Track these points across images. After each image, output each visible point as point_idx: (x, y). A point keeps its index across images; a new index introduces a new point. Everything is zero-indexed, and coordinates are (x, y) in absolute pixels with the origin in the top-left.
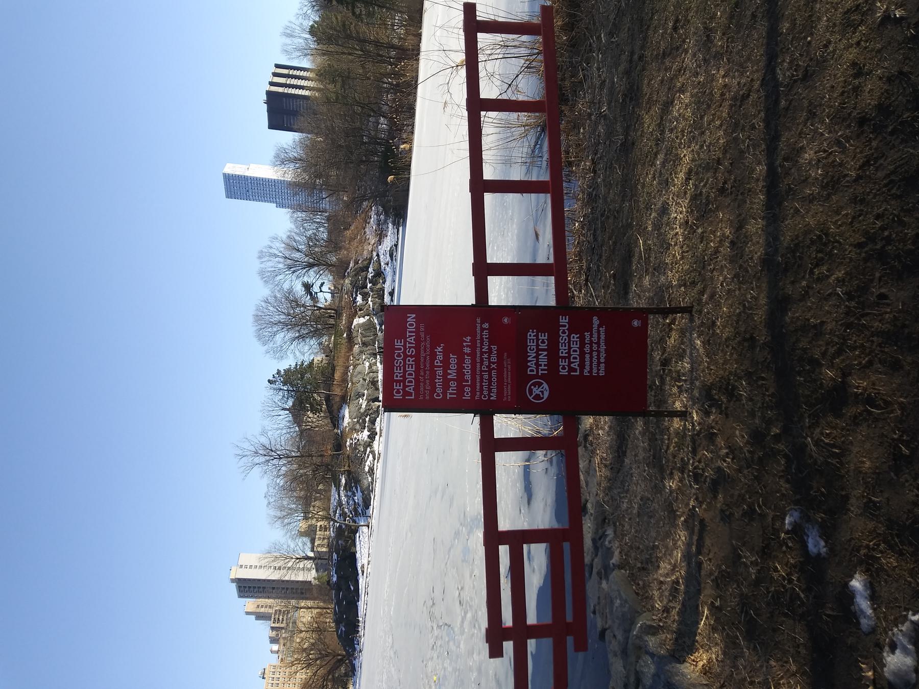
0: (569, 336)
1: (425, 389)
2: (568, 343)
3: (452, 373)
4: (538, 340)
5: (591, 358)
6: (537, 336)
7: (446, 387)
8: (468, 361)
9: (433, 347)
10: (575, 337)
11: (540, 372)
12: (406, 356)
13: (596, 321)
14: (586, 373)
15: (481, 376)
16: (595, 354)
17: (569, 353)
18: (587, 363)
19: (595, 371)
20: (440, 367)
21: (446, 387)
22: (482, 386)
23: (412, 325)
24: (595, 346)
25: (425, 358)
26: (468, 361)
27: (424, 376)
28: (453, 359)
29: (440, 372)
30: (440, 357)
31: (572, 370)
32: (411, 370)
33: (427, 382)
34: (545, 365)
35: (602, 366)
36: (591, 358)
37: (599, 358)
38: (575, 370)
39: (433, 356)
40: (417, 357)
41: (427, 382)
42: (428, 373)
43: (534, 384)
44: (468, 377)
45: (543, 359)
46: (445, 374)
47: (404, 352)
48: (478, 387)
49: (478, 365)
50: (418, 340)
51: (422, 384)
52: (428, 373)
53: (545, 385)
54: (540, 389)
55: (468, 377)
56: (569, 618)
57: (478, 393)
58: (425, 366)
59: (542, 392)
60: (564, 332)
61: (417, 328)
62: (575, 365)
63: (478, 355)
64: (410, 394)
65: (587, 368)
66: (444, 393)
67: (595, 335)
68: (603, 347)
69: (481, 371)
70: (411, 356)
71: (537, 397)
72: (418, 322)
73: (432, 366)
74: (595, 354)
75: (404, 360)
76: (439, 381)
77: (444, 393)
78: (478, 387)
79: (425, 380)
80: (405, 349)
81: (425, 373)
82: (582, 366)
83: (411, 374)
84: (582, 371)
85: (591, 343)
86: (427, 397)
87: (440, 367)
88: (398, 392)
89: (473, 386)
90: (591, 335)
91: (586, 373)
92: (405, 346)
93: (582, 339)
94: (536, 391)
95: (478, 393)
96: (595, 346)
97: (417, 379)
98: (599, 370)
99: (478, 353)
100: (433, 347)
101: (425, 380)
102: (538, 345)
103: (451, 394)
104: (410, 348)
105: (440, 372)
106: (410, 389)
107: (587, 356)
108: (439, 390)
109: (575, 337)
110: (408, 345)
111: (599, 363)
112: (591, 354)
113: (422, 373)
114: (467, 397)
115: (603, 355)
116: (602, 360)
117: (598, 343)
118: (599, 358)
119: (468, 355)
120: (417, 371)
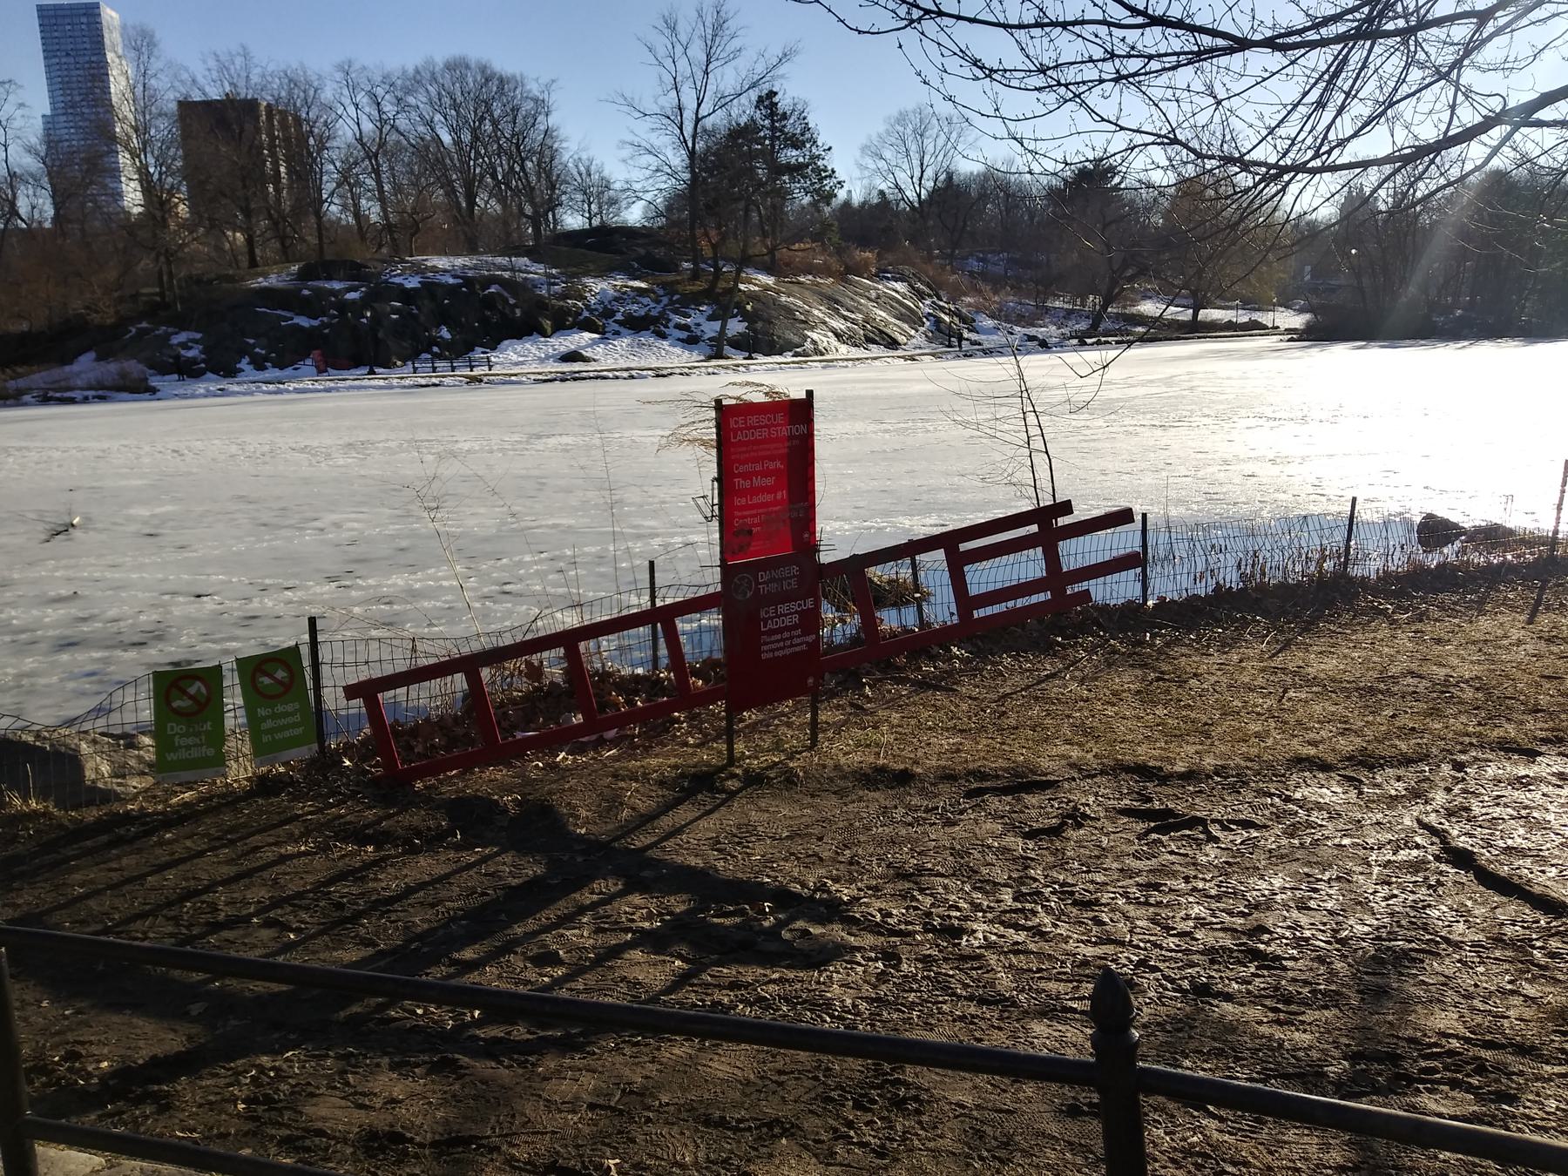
3: (758, 482)
8: (768, 498)
18: (773, 638)
26: (768, 498)
28: (770, 481)
29: (758, 467)
30: (772, 466)
31: (766, 621)
39: (772, 459)
44: (756, 500)
46: (756, 474)
55: (756, 500)
56: (1034, 528)
62: (770, 625)
67: (799, 641)
68: (787, 652)
85: (791, 638)
108: (742, 469)
117: (792, 646)
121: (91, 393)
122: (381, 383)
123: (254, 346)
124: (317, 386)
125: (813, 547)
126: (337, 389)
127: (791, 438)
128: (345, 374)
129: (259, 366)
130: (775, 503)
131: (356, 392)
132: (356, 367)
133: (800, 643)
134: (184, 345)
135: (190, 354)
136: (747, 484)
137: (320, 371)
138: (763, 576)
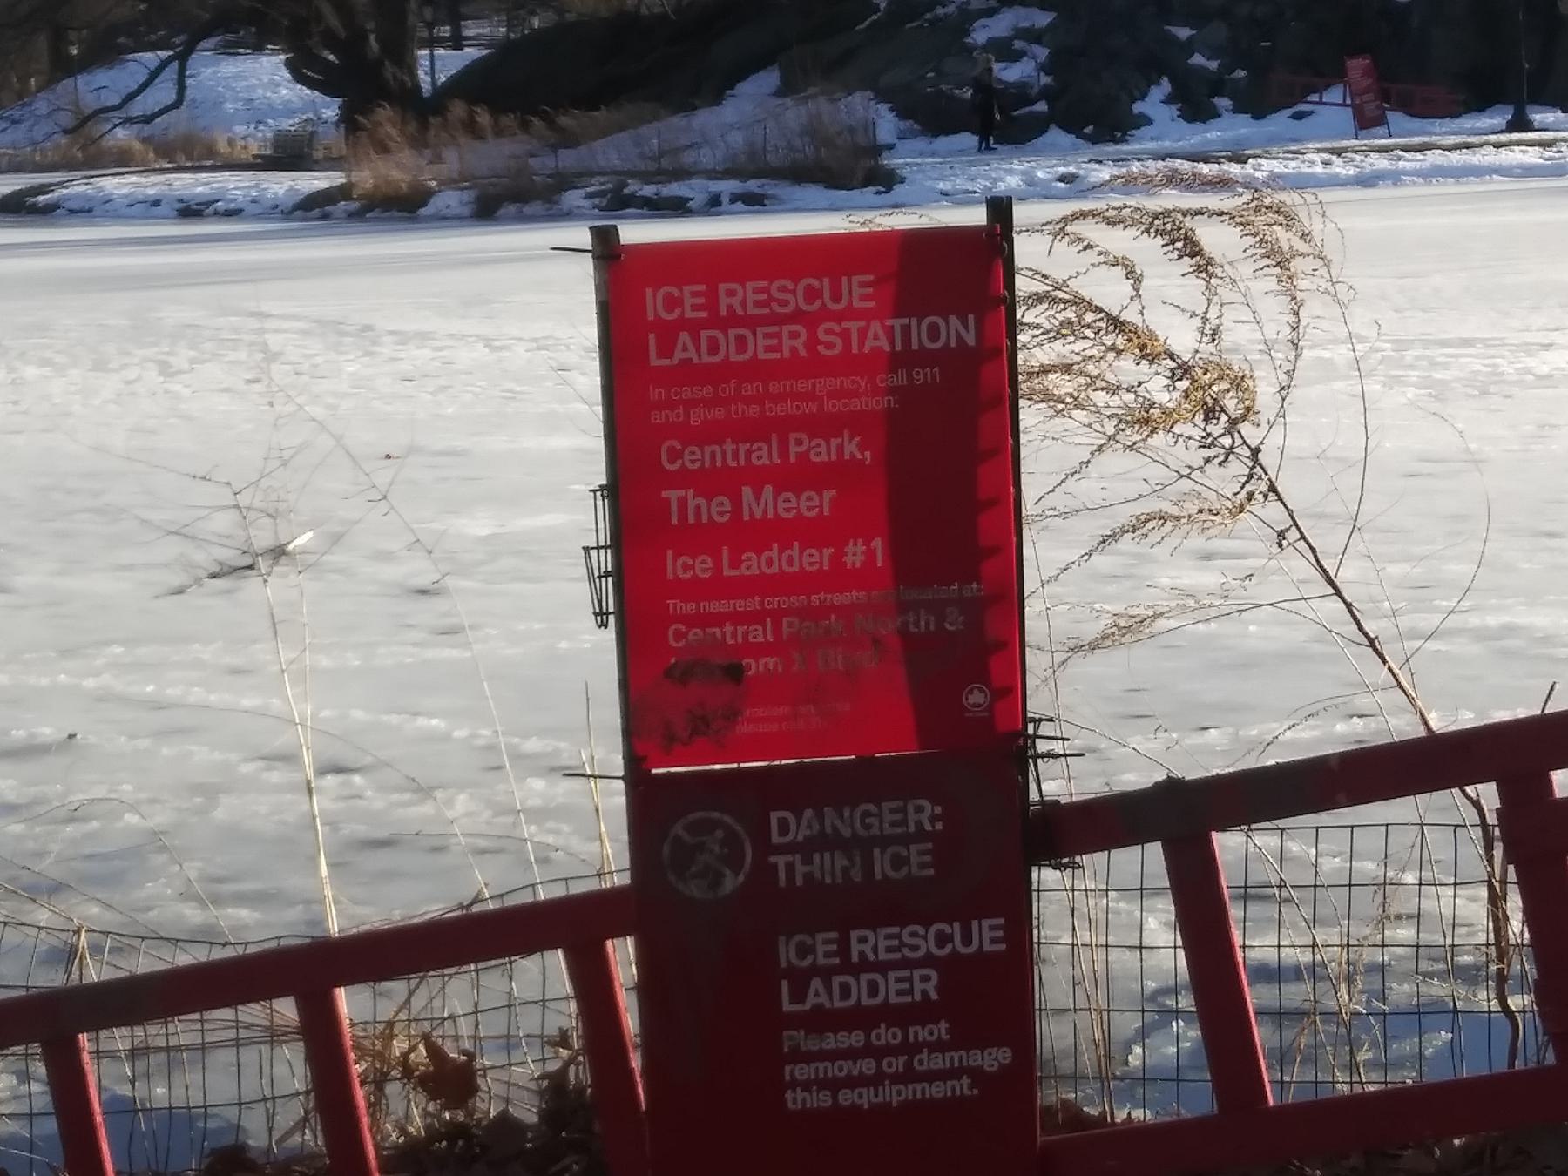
0: (929, 961)
1: (690, 404)
2: (900, 962)
3: (760, 504)
4: (906, 840)
5: (852, 1054)
6: (921, 835)
7: (710, 482)
8: (814, 559)
9: (855, 423)
10: (927, 984)
11: (781, 861)
12: (810, 321)
13: (994, 1059)
14: (794, 1037)
15: (756, 618)
16: (867, 1066)
17: (865, 966)
18: (832, 1042)
19: (802, 1072)
20: (784, 452)
21: (710, 482)
22: (718, 620)
23: (934, 333)
24: (897, 1064)
25: (810, 397)
28: (814, 504)
29: (764, 455)
30: (822, 452)
32: (759, 345)
34: (808, 877)
35: (822, 1100)
36: (852, 1054)
37: (852, 1082)
38: (799, 995)
40: (812, 365)
42: (753, 411)
44: (752, 565)
45: (830, 867)
48: (714, 607)
49: (796, 601)
55: (752, 565)
57: (691, 608)
60: (942, 939)
61: (925, 358)
63: (837, 599)
65: (811, 1044)
66: (683, 479)
67: (939, 1062)
68: (894, 1095)
69: (777, 615)
70: (813, 343)
73: (784, 427)
74: (867, 1066)
75: (797, 316)
76: (727, 454)
77: (683, 479)
78: (714, 607)
80: (839, 317)
81: (748, 400)
82: (822, 1021)
84: (797, 1021)
85: (910, 1049)
87: (784, 452)
89: (718, 587)
90: (939, 1047)
91: (794, 1037)
92: (850, 313)
93: (922, 1012)
95: (691, 608)
96: (897, 1064)
97: (725, 372)
98: (806, 1086)
99: (837, 599)
100: (855, 423)
102: (884, 841)
103: (683, 503)
104: (845, 335)
105: (764, 455)
106: (685, 349)
107: (856, 1039)
108: (694, 458)
109: (927, 984)
110: (854, 326)
111: (834, 1085)
112: (869, 1051)
113: (750, 389)
114: (677, 567)
115: (865, 1098)
116: (846, 1097)
118: (852, 1082)
119: (837, 559)
120: (755, 370)
121: (728, 186)
122: (1533, 156)
123: (1189, 47)
124: (1340, 168)
125: (1010, 745)
126: (1395, 178)
127: (903, 359)
128: (1444, 131)
129: (1195, 105)
130: (839, 577)
131: (1450, 187)
132: (1480, 104)
133: (949, 1071)
134: (1005, 50)
135: (1011, 73)
136: (718, 510)
137: (1366, 122)
138: (791, 826)
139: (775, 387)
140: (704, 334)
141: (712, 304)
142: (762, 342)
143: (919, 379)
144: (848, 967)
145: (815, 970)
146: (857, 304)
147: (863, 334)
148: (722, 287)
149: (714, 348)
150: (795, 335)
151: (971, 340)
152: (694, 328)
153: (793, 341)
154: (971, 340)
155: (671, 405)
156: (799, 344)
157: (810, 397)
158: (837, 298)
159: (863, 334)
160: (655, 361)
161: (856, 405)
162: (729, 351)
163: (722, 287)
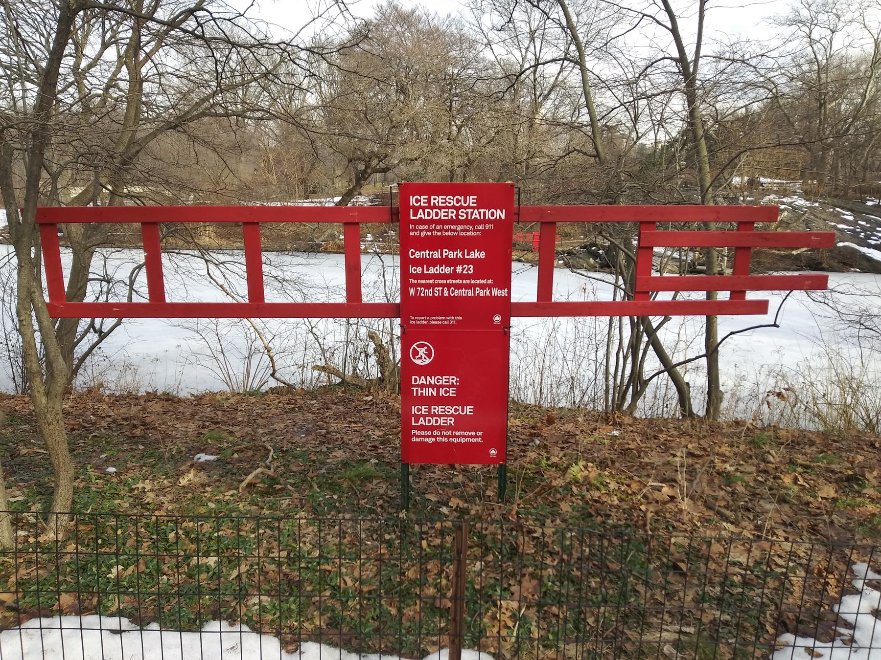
1: (421, 230)
12: (457, 209)
23: (493, 214)
25: (455, 230)
27: (435, 229)
32: (442, 215)
33: (429, 233)
40: (457, 222)
41: (429, 233)
42: (439, 234)
43: (429, 350)
47: (461, 207)
50: (475, 222)
51: (426, 227)
52: (439, 234)
53: (428, 361)
54: (424, 356)
58: (446, 231)
59: (421, 358)
61: (489, 221)
64: (415, 215)
71: (416, 353)
72: (496, 222)
75: (453, 207)
79: (431, 231)
80: (465, 208)
81: (438, 231)
83: (437, 216)
86: (412, 234)
88: (417, 201)
92: (469, 207)
94: (422, 351)
97: (432, 221)
101: (431, 231)
104: (467, 213)
106: (421, 215)
110: (470, 211)
113: (438, 227)
139: (446, 227)
140: (426, 211)
141: (429, 202)
142: (443, 214)
143: (487, 228)
144: (430, 415)
145: (421, 415)
146: (471, 205)
147: (472, 213)
148: (432, 197)
149: (429, 216)
150: (452, 212)
151: (503, 218)
152: (424, 208)
153: (452, 214)
154: (503, 218)
155: (416, 231)
156: (453, 215)
157: (455, 230)
158: (465, 202)
159: (472, 213)
160: (412, 218)
161: (469, 234)
162: (433, 215)
163: (432, 197)
